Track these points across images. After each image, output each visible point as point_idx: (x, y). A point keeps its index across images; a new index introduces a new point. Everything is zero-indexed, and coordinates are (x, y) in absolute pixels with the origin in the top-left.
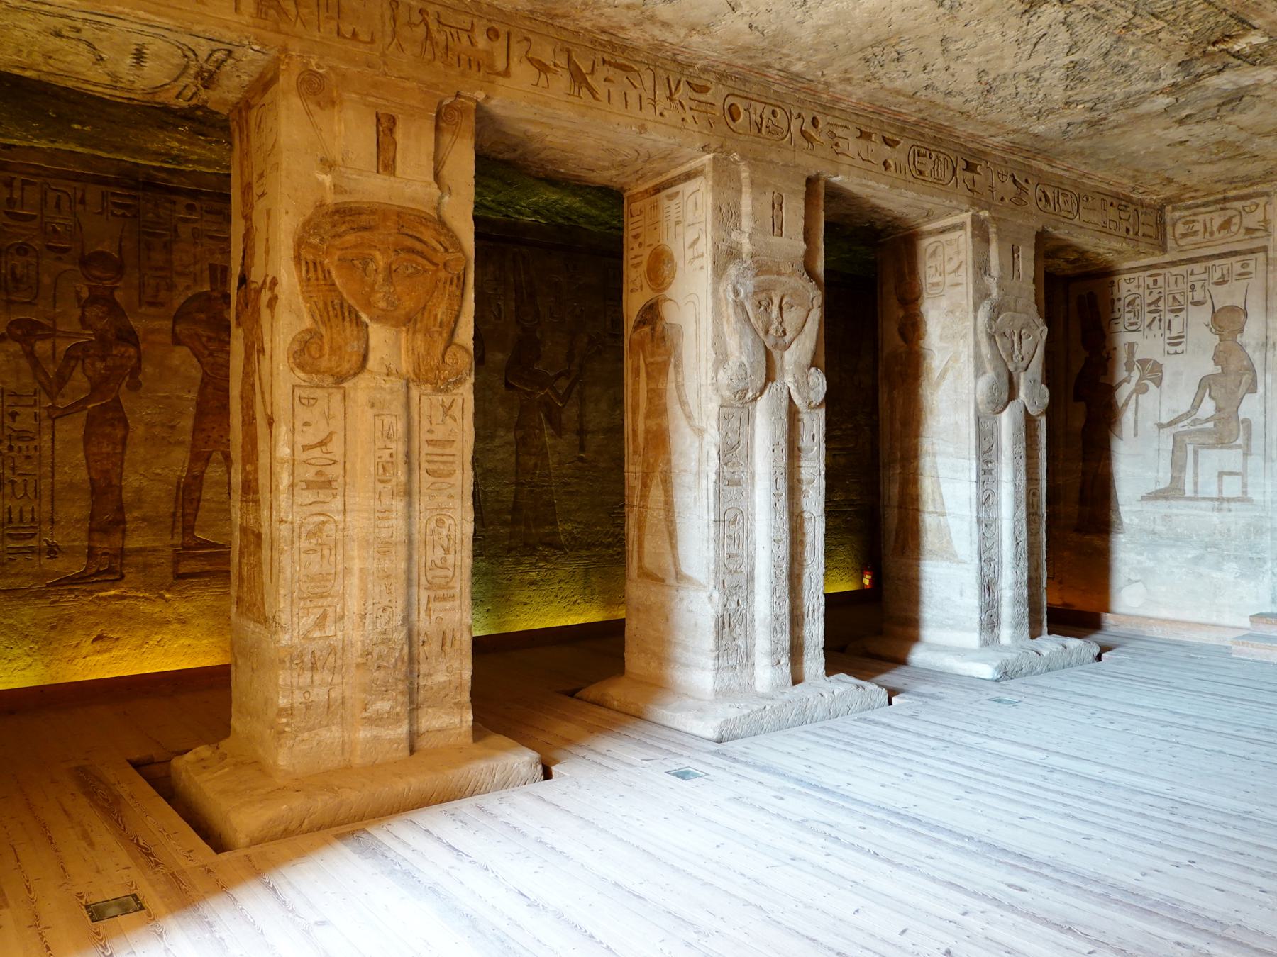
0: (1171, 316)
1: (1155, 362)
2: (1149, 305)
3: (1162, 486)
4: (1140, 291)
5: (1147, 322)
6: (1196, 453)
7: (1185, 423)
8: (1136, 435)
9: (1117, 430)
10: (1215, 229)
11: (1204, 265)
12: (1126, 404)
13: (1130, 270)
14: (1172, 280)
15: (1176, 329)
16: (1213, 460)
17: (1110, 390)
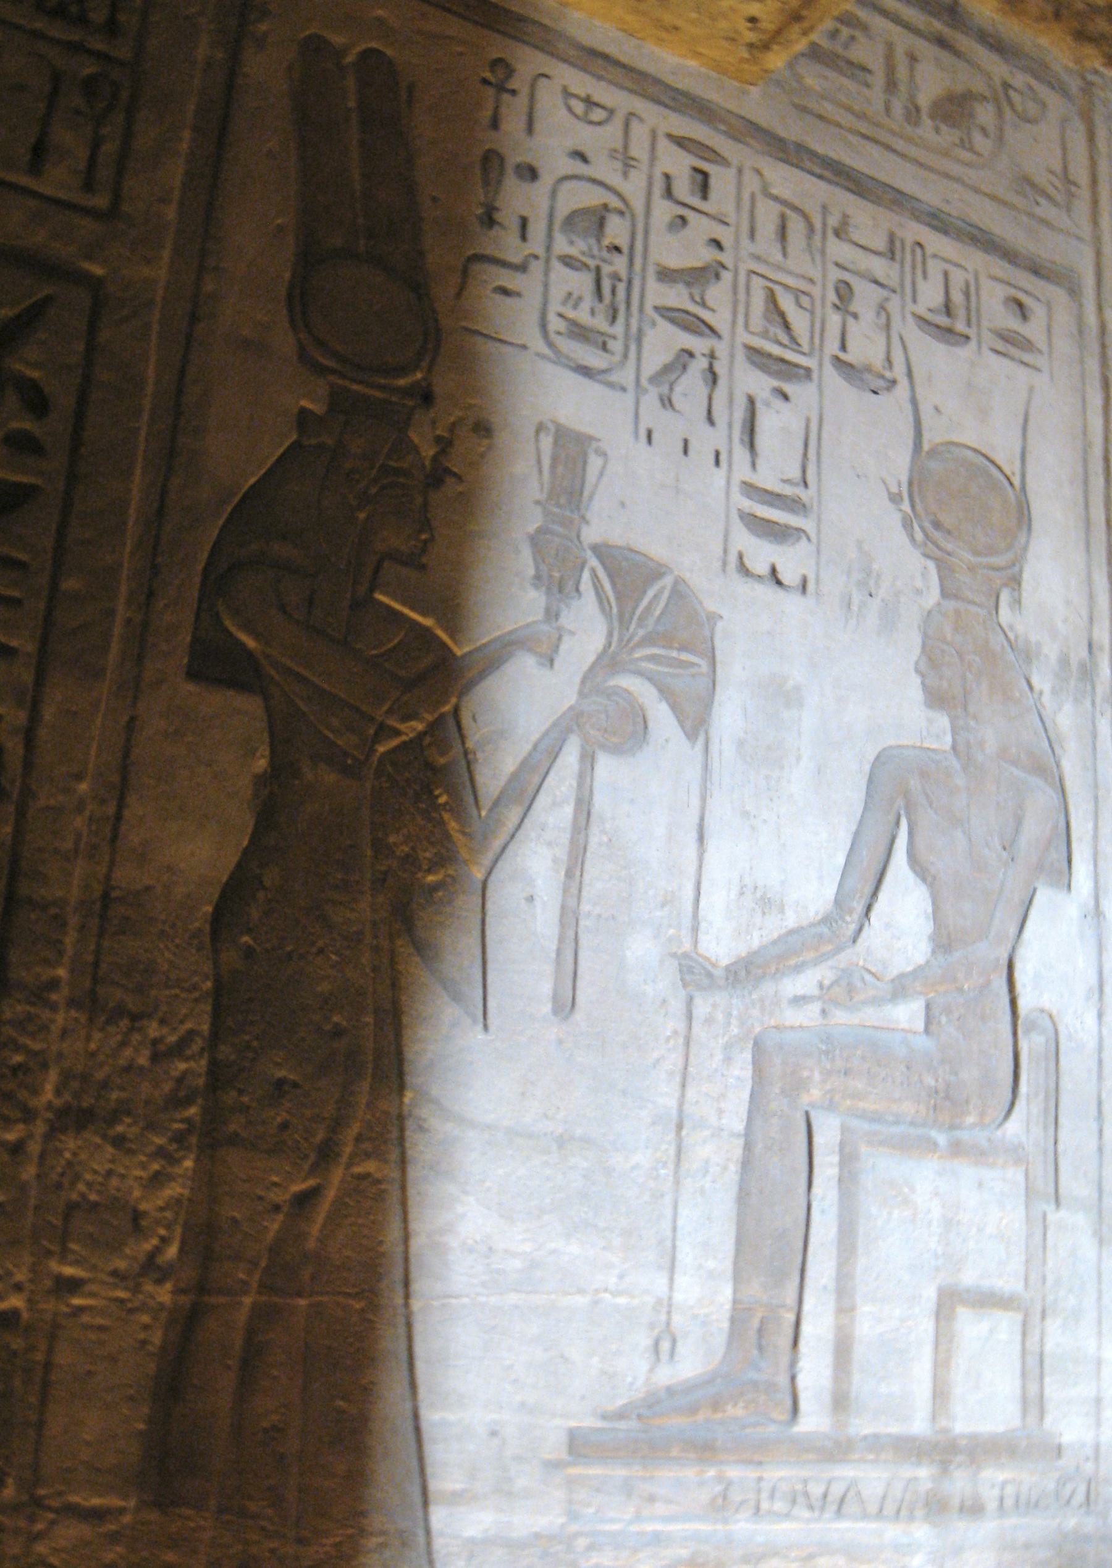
0: (759, 383)
1: (680, 593)
2: (666, 275)
3: (689, 1365)
4: (633, 187)
5: (655, 356)
6: (848, 1158)
7: (805, 983)
8: (565, 1005)
9: (458, 949)
10: (924, 101)
11: (888, 219)
12: (524, 790)
13: (594, 59)
14: (767, 215)
15: (776, 467)
16: (927, 1218)
17: (433, 675)
